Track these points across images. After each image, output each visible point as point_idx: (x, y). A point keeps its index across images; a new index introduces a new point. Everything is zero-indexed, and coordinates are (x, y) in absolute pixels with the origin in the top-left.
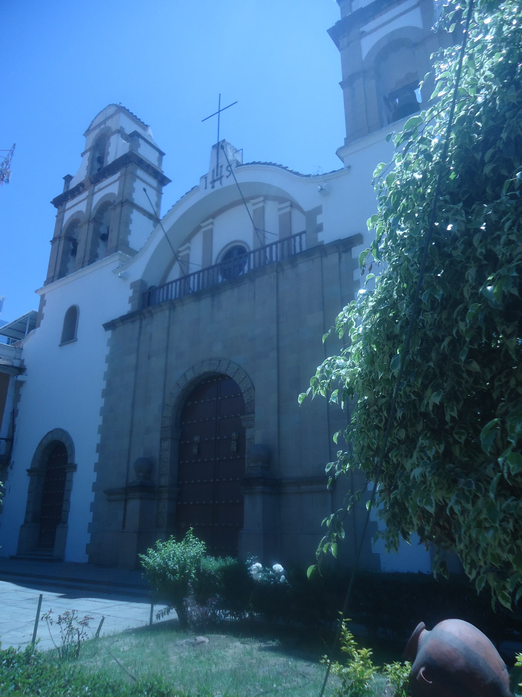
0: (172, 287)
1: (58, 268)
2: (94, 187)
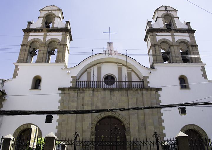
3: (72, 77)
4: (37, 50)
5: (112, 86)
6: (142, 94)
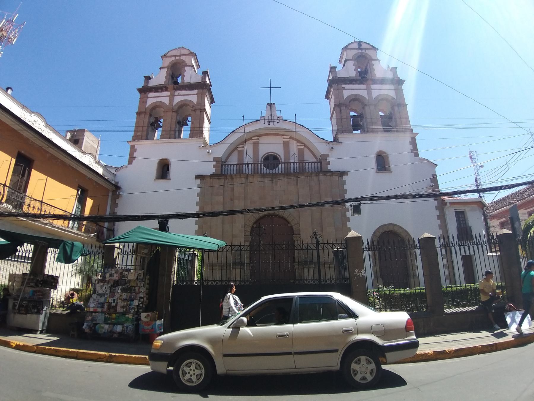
2: (175, 91)
3: (215, 159)
4: (162, 121)
5: (274, 170)
6: (319, 180)
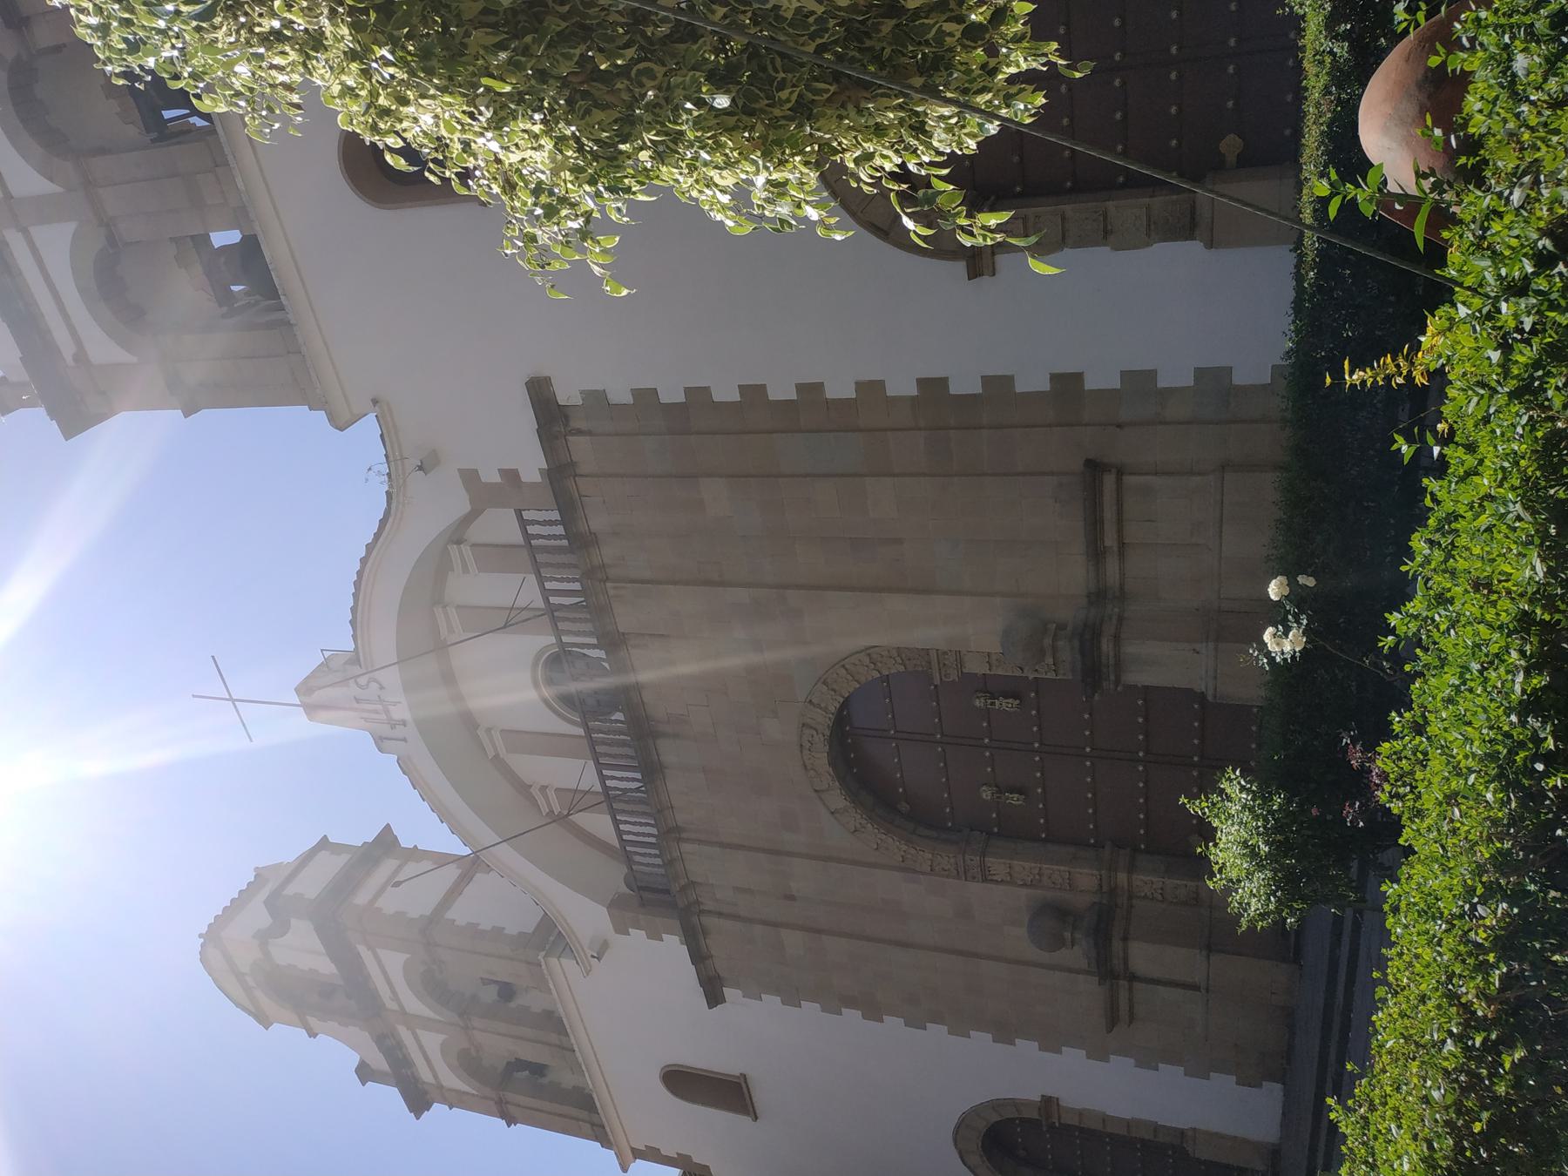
0: (629, 833)
1: (574, 1112)
3: (621, 929)
